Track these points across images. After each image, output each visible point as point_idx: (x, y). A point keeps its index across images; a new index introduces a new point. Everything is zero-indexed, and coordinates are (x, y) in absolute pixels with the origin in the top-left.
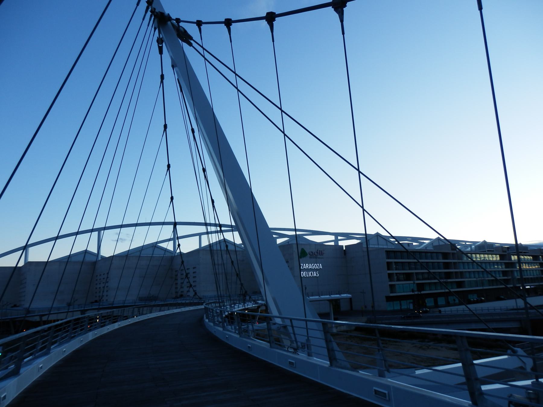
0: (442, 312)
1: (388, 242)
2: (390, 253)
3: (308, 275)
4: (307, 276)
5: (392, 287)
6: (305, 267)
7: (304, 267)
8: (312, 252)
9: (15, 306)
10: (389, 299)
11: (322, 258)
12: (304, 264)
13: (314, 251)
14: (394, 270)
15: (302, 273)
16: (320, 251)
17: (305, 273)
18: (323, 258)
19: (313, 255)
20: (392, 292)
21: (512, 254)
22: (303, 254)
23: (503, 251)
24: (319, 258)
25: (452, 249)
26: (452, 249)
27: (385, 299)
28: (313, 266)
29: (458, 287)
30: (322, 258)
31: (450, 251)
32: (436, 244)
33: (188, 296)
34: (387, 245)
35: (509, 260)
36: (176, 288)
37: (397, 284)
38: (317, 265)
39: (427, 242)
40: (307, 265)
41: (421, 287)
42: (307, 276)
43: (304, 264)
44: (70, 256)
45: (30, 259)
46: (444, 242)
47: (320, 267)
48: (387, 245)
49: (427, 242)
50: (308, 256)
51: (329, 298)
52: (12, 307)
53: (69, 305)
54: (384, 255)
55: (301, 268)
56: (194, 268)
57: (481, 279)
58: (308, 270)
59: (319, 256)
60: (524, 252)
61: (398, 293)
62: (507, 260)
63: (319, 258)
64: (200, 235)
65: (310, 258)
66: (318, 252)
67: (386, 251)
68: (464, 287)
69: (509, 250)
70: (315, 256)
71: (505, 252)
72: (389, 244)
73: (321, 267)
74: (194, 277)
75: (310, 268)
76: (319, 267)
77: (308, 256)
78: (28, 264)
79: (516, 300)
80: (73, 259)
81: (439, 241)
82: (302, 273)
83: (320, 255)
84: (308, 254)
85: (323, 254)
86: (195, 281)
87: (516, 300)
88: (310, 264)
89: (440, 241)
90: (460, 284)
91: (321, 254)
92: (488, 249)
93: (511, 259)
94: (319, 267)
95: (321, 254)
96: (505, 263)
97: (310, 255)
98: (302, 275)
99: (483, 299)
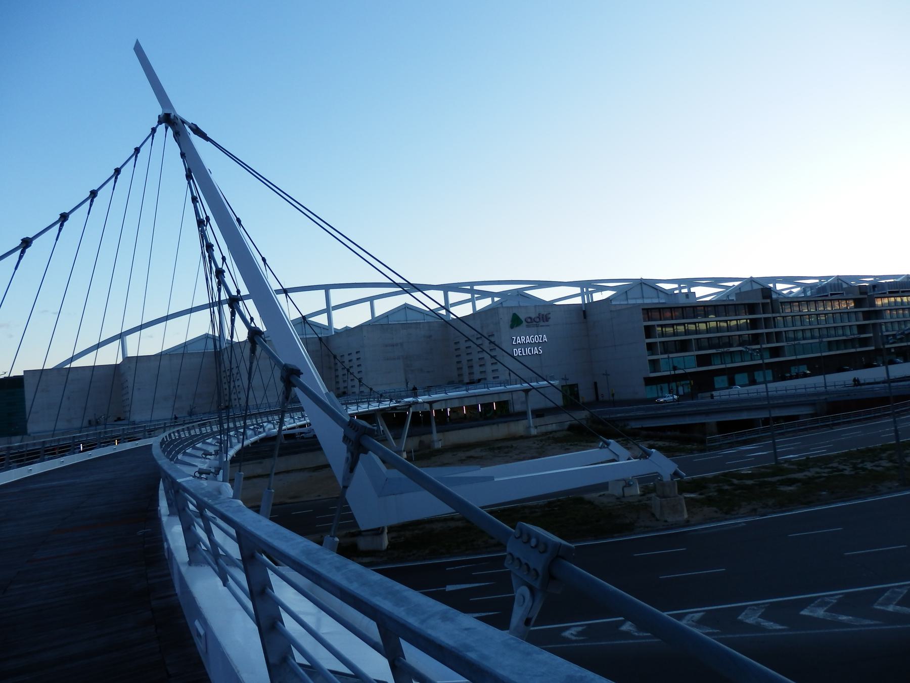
0: (715, 397)
1: (659, 292)
2: (648, 312)
3: (525, 353)
4: (523, 354)
5: (654, 364)
6: (520, 342)
7: (518, 342)
8: (530, 318)
9: (119, 419)
10: (649, 381)
11: (547, 326)
12: (518, 337)
13: (533, 316)
14: (657, 337)
15: (515, 351)
16: (543, 315)
17: (520, 350)
18: (549, 326)
19: (532, 322)
20: (655, 371)
21: (875, 296)
22: (516, 321)
23: (861, 293)
24: (541, 326)
25: (764, 298)
26: (764, 298)
27: (643, 382)
28: (533, 339)
29: (772, 357)
30: (547, 326)
31: (761, 301)
32: (747, 288)
33: (353, 393)
34: (658, 297)
35: (871, 306)
36: (337, 382)
37: (662, 359)
38: (540, 337)
39: (736, 283)
40: (523, 338)
41: (702, 360)
42: (523, 354)
43: (518, 337)
44: (185, 345)
45: (131, 353)
46: (762, 285)
47: (544, 340)
48: (658, 297)
49: (736, 283)
50: (524, 323)
51: (520, 387)
52: (115, 421)
53: (191, 414)
54: (641, 316)
55: (514, 343)
56: (357, 352)
57: (853, 337)
58: (524, 345)
59: (542, 323)
60: (903, 292)
61: (663, 371)
62: (867, 307)
63: (541, 326)
64: (371, 299)
65: (528, 326)
66: (541, 318)
67: (643, 309)
68: (784, 356)
69: (876, 289)
70: (535, 323)
71: (866, 293)
72: (661, 295)
73: (546, 340)
74: (359, 366)
75: (528, 342)
76: (542, 339)
77: (524, 323)
78: (127, 359)
79: (824, 377)
80: (190, 350)
81: (751, 284)
82: (515, 351)
83: (543, 321)
84: (523, 320)
85: (549, 318)
86: (361, 371)
87: (824, 377)
88: (527, 337)
89: (754, 283)
90: (776, 352)
91: (545, 320)
92: (832, 291)
93: (874, 305)
94: (542, 339)
95: (545, 320)
96: (863, 312)
97: (528, 322)
98: (516, 354)
99: (808, 372)
